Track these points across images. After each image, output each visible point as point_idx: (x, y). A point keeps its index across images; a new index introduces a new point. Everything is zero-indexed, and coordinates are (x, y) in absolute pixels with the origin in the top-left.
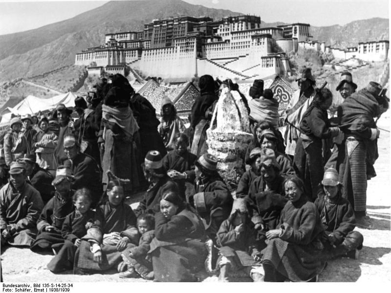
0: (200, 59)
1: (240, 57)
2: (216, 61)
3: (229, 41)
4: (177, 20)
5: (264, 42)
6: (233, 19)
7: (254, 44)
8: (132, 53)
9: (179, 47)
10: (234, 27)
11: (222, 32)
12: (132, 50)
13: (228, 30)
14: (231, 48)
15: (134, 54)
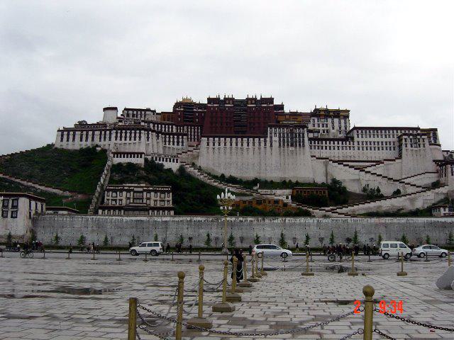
0: (317, 158)
1: (385, 160)
2: (350, 164)
3: (352, 139)
4: (253, 102)
5: (424, 145)
6: (332, 114)
7: (409, 146)
8: (178, 138)
9: (276, 139)
10: (333, 122)
11: (316, 127)
12: (178, 135)
13: (327, 125)
14: (356, 148)
15: (180, 140)
